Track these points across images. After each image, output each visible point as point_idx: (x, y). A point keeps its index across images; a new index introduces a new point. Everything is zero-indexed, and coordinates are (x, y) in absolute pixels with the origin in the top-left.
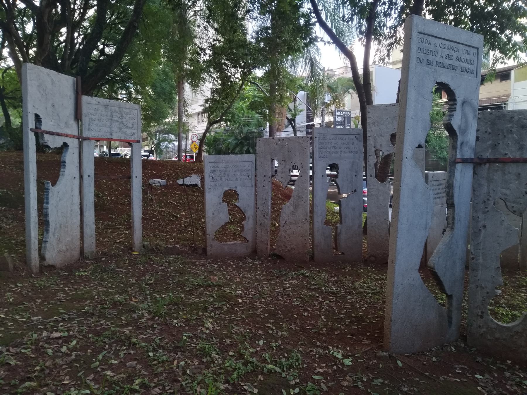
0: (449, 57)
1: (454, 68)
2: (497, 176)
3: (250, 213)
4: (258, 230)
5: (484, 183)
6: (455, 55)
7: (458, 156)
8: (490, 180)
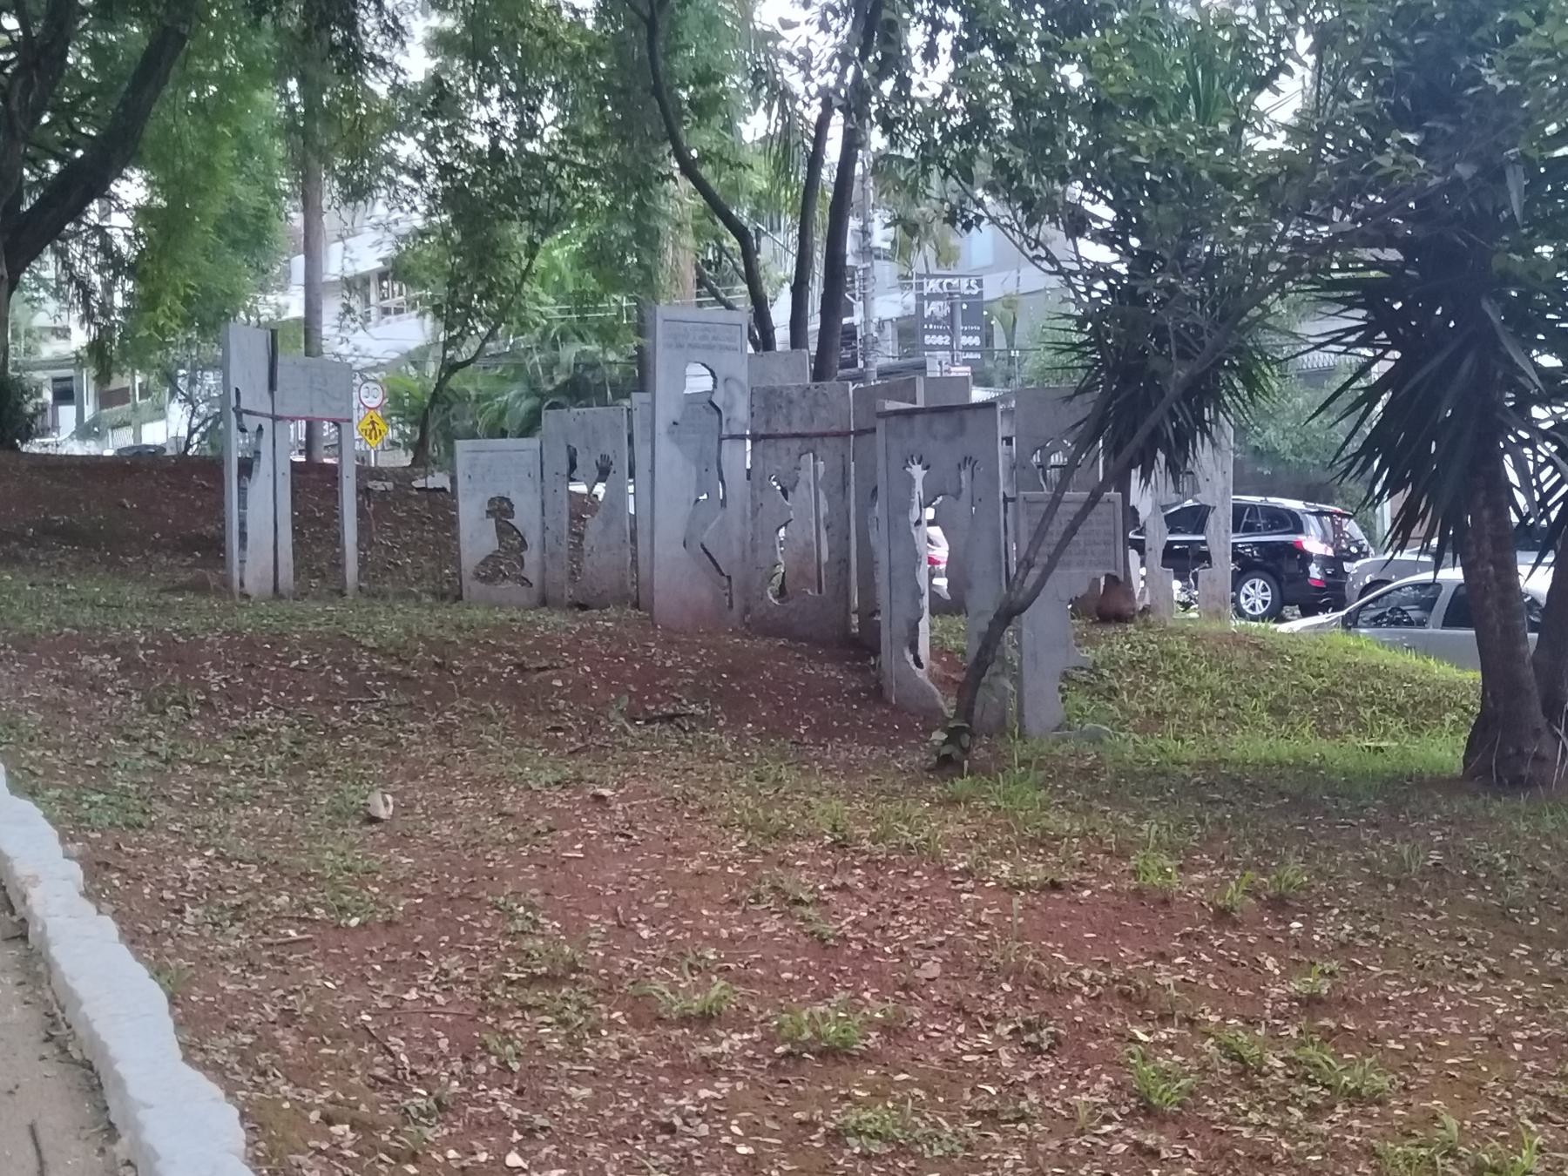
0: (704, 337)
1: (710, 347)
2: (771, 452)
3: (533, 538)
4: (548, 565)
5: (760, 459)
6: (710, 335)
7: (725, 432)
8: (764, 456)
